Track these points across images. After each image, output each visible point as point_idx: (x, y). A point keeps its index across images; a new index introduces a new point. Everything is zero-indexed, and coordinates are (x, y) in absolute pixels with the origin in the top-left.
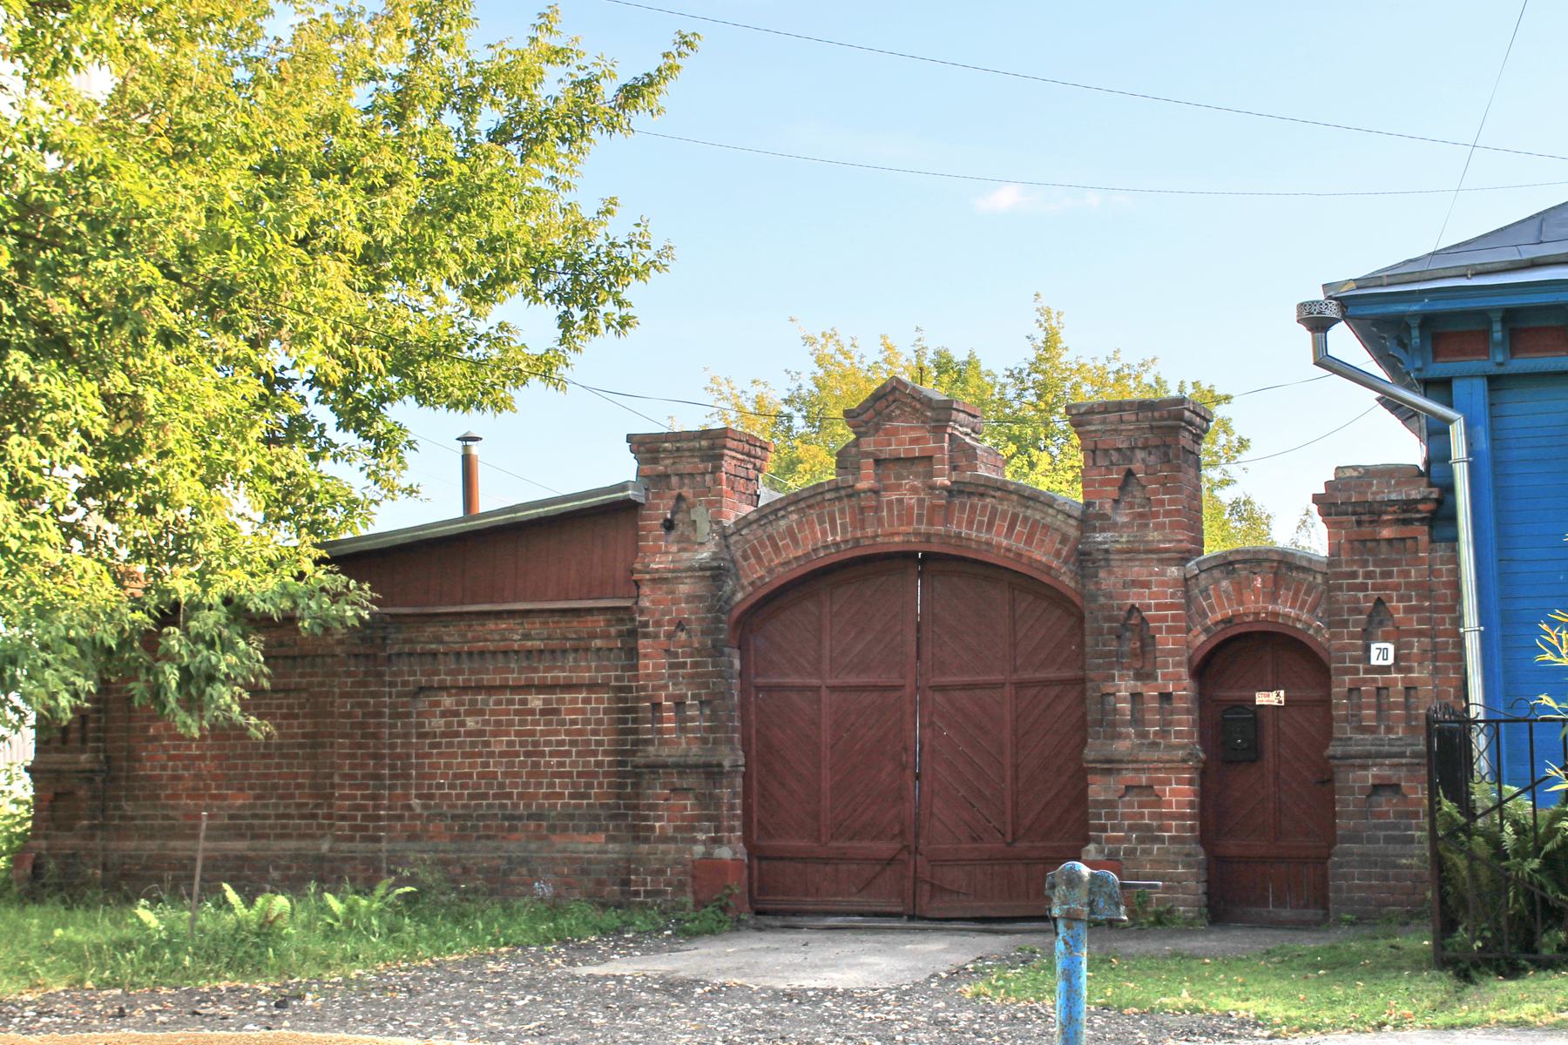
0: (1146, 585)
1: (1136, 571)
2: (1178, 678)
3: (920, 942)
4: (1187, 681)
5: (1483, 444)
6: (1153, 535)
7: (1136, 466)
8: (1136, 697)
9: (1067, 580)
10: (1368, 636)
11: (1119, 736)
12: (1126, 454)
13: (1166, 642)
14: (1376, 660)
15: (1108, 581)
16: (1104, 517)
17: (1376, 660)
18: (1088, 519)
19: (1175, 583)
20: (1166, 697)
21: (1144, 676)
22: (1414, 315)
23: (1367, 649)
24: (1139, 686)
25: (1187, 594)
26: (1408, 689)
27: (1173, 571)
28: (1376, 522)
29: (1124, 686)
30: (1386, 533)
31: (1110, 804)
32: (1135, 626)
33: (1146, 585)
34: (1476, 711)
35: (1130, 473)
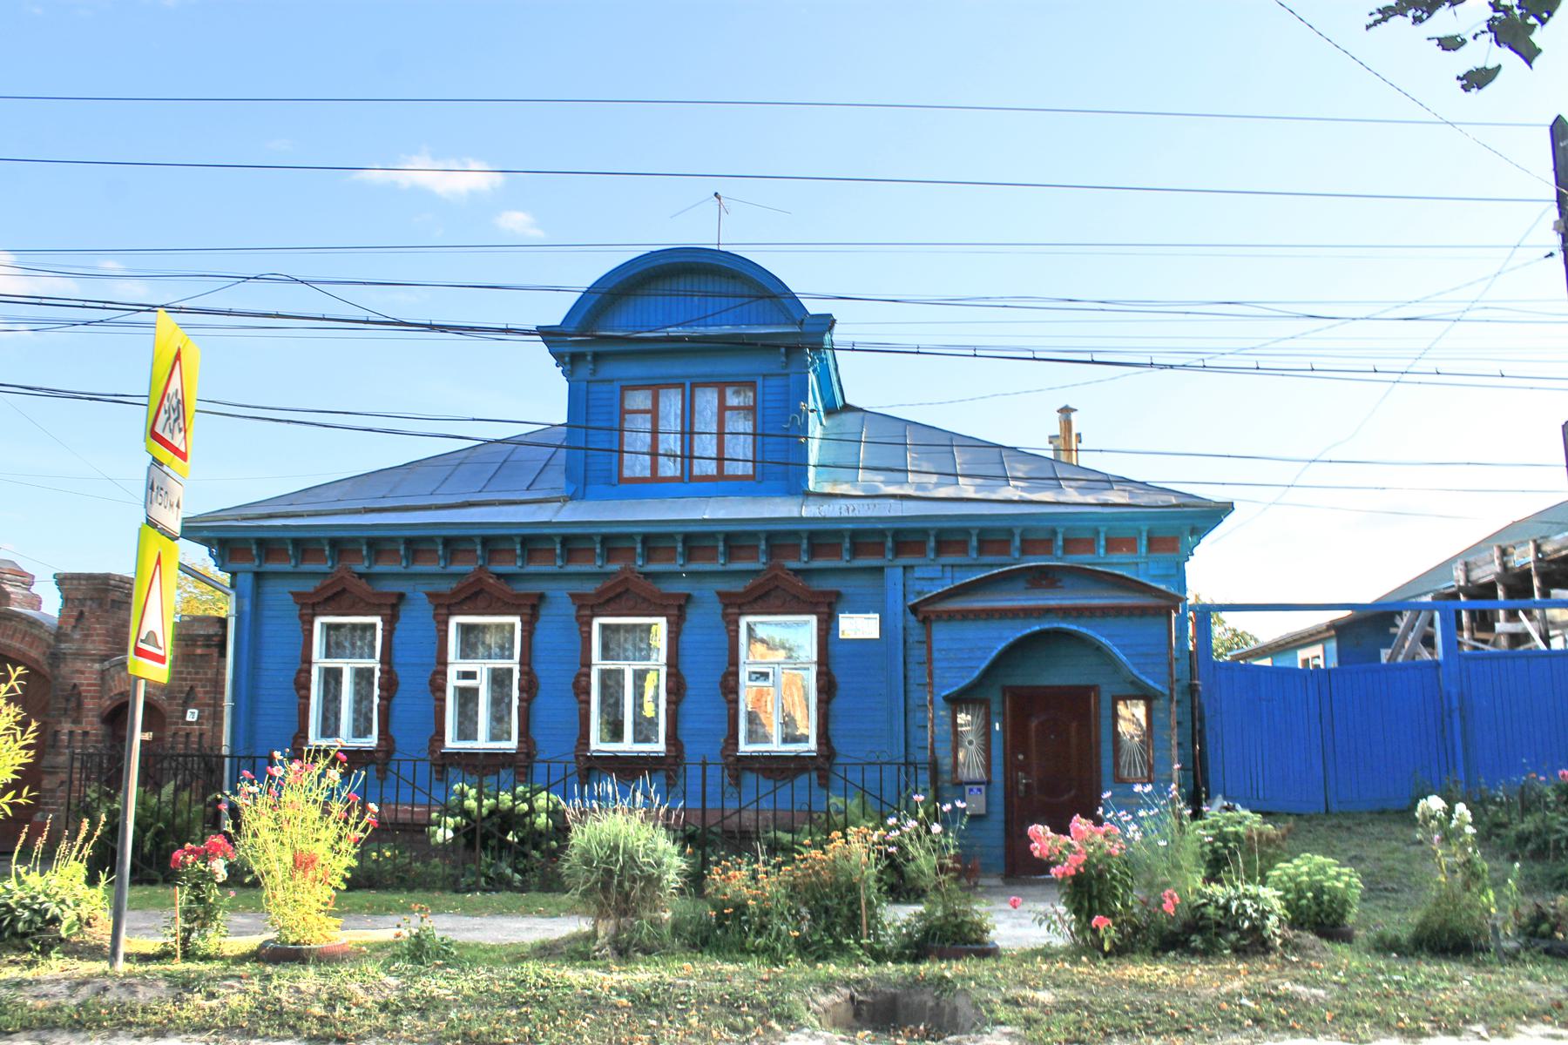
0: (82, 673)
1: (79, 665)
2: (92, 724)
3: (472, 911)
4: (98, 726)
5: (247, 607)
6: (89, 646)
7: (86, 609)
8: (71, 733)
9: (47, 668)
10: (186, 705)
11: (60, 754)
12: (82, 601)
13: (89, 704)
14: (189, 718)
15: (65, 669)
16: (66, 635)
17: (189, 718)
18: (60, 635)
19: (97, 672)
20: (86, 734)
21: (76, 721)
22: (638, 534)
23: (185, 713)
24: (73, 727)
25: (103, 679)
26: (201, 735)
27: (97, 666)
28: (195, 645)
29: (66, 727)
30: (199, 651)
31: (52, 790)
32: (75, 695)
33: (82, 673)
34: (225, 751)
35: (81, 614)
